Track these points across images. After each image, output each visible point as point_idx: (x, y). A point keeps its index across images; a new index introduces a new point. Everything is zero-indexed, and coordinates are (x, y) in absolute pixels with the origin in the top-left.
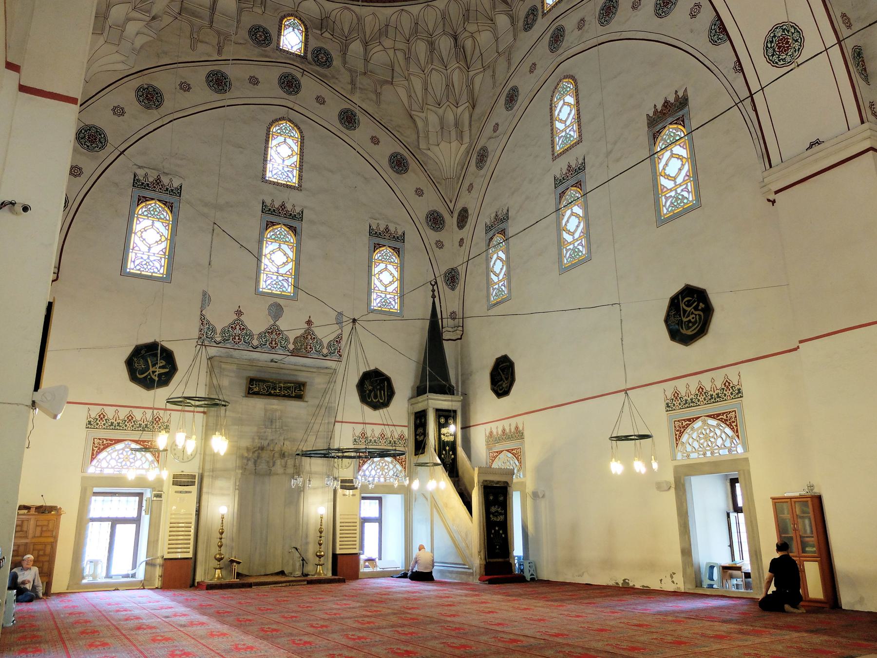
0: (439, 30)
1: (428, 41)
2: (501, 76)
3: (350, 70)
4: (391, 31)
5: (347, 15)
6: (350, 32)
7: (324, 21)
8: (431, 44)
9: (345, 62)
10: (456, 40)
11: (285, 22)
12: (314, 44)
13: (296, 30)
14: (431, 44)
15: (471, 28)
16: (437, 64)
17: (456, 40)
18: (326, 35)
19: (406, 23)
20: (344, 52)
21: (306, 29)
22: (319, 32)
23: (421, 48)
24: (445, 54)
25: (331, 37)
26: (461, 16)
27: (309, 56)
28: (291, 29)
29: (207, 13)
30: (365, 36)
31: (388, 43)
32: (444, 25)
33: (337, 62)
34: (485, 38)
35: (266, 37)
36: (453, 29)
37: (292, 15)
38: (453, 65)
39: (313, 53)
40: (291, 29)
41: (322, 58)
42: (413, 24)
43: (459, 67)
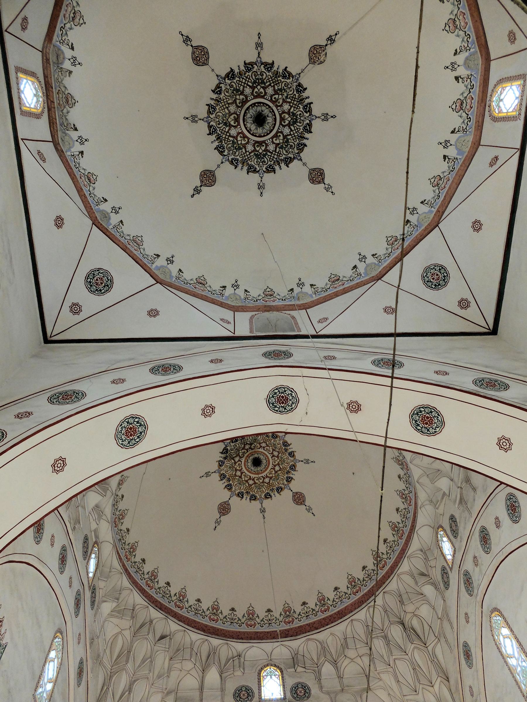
0: (387, 623)
1: (382, 637)
2: (451, 637)
3: (328, 693)
4: (350, 641)
5: (312, 646)
6: (318, 659)
7: (295, 659)
8: (385, 637)
9: (321, 688)
10: (403, 624)
11: (263, 674)
12: (290, 682)
13: (273, 677)
14: (385, 637)
15: (410, 608)
16: (397, 654)
17: (403, 624)
18: (300, 669)
19: (361, 630)
20: (319, 679)
21: (282, 672)
22: (293, 670)
23: (379, 645)
24: (400, 641)
25: (304, 670)
26: (398, 602)
27: (289, 695)
28: (269, 677)
29: (197, 694)
30: (331, 655)
31: (351, 653)
32: (388, 616)
33: (314, 690)
34: (425, 611)
35: (248, 694)
36: (397, 617)
37: (267, 665)
38: (410, 647)
39: (291, 691)
40: (269, 677)
41: (301, 692)
42: (365, 627)
43: (414, 648)
